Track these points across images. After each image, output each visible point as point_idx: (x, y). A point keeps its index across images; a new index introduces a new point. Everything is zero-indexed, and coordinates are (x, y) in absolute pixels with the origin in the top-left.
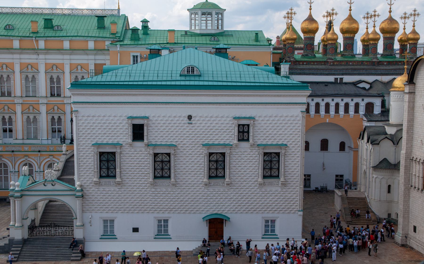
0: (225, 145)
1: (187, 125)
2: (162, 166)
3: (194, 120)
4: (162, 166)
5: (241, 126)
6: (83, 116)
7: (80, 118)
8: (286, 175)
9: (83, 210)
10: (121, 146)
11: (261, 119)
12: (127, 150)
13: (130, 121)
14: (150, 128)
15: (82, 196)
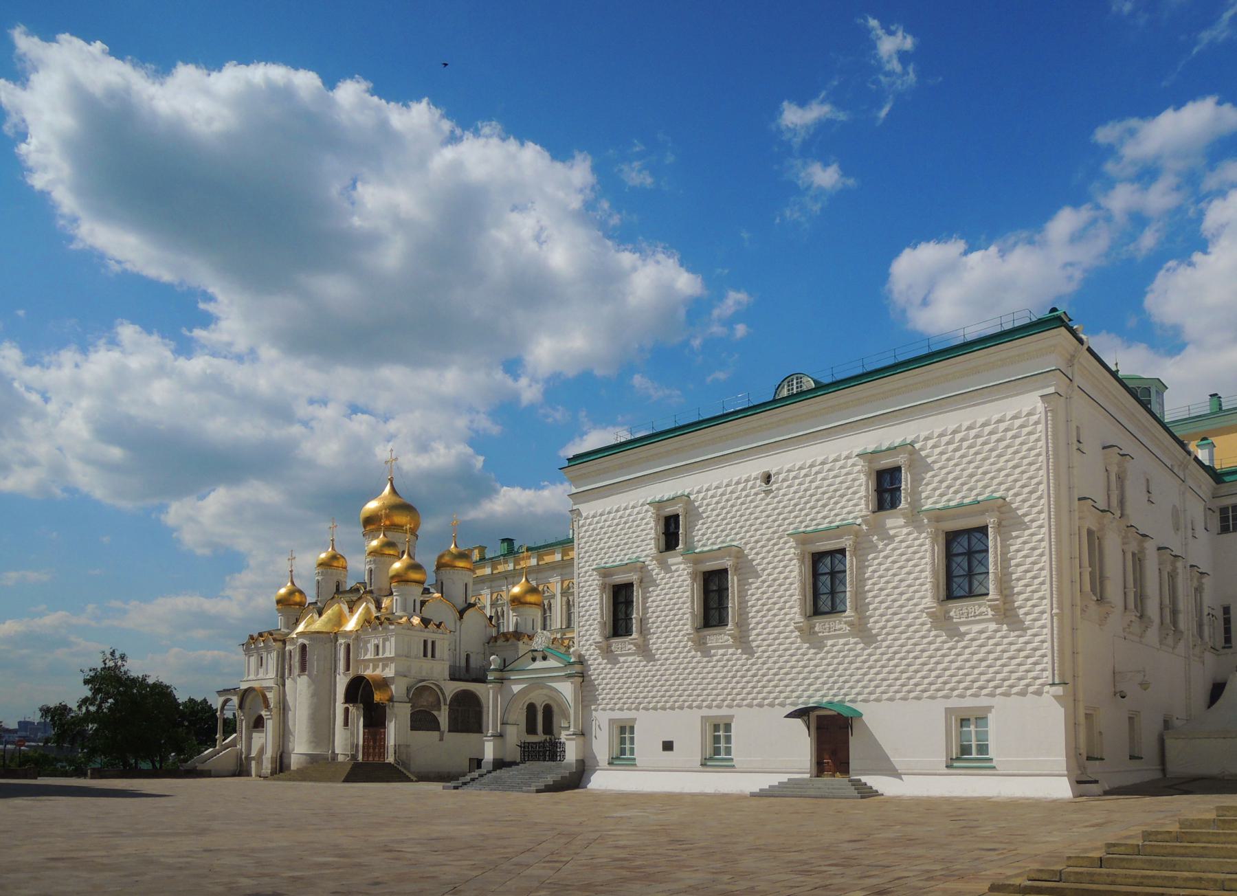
2: (714, 598)
3: (775, 482)
4: (714, 598)
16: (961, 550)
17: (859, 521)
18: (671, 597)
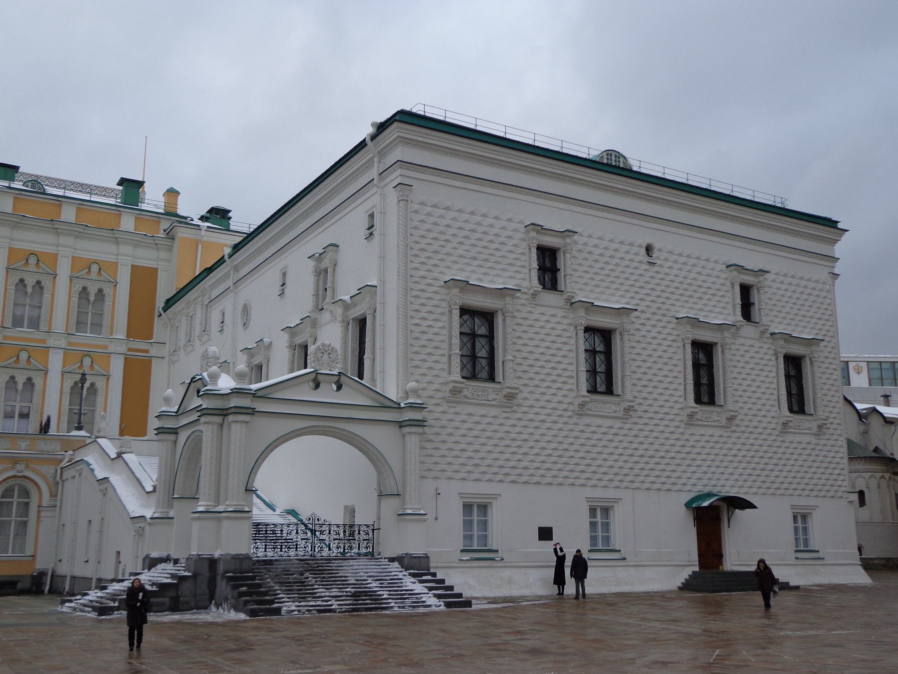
1: (646, 267)
3: (658, 258)
13: (534, 234)
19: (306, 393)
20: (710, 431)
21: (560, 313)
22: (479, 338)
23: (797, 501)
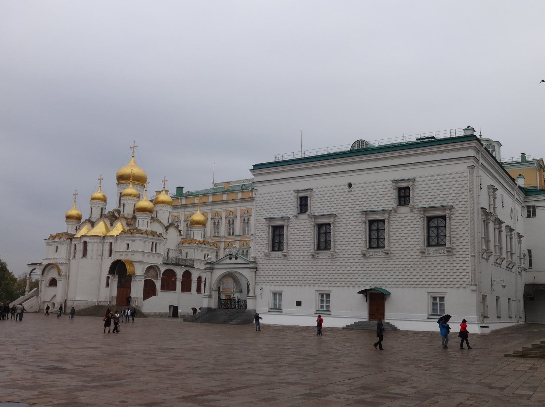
0: (383, 212)
1: (347, 193)
3: (353, 188)
5: (403, 191)
6: (261, 194)
7: (258, 196)
8: (452, 242)
9: (255, 283)
10: (288, 218)
11: (422, 179)
12: (293, 223)
14: (314, 199)
15: (256, 268)
16: (434, 225)
17: (391, 209)
18: (301, 234)
19: (228, 261)
20: (376, 260)
21: (307, 221)
22: (278, 235)
23: (431, 290)
